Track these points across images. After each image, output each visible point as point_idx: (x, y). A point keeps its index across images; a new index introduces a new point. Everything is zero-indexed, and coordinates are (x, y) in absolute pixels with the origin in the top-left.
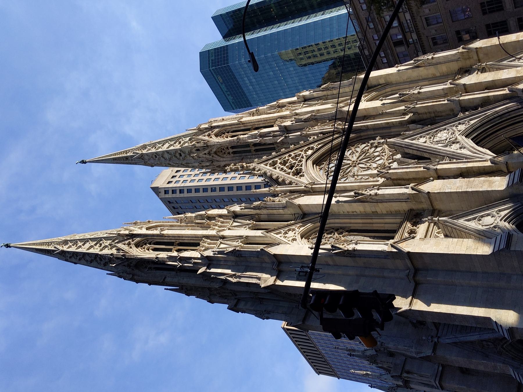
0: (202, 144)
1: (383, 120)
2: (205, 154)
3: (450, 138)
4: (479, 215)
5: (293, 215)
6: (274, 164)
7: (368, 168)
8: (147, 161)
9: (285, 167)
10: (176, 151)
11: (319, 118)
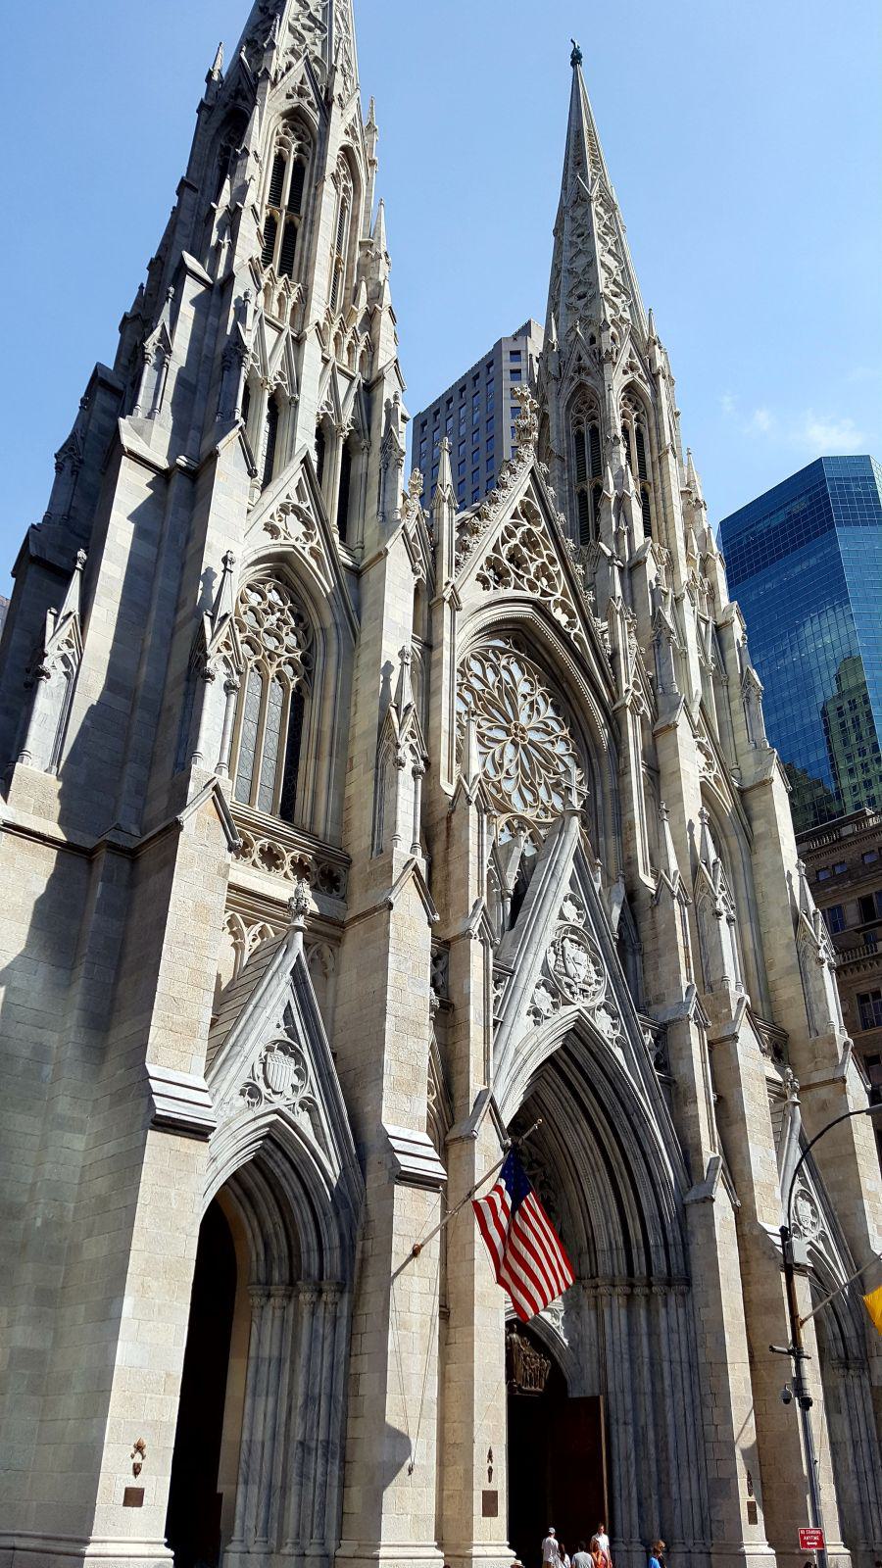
0: (606, 344)
1: (641, 814)
2: (580, 359)
3: (569, 986)
4: (305, 1048)
5: (359, 544)
6: (526, 512)
7: (501, 765)
8: (570, 213)
9: (517, 542)
10: (594, 283)
11: (662, 650)
